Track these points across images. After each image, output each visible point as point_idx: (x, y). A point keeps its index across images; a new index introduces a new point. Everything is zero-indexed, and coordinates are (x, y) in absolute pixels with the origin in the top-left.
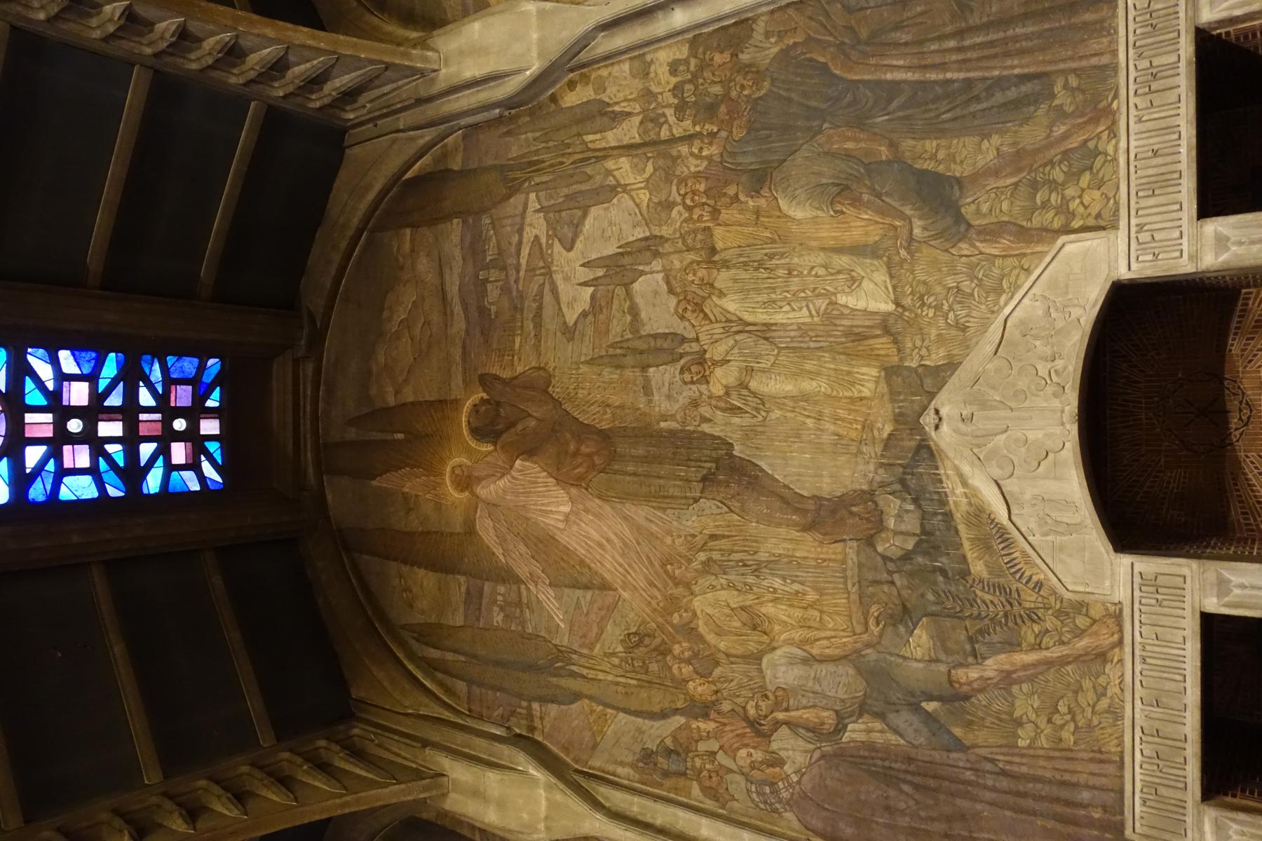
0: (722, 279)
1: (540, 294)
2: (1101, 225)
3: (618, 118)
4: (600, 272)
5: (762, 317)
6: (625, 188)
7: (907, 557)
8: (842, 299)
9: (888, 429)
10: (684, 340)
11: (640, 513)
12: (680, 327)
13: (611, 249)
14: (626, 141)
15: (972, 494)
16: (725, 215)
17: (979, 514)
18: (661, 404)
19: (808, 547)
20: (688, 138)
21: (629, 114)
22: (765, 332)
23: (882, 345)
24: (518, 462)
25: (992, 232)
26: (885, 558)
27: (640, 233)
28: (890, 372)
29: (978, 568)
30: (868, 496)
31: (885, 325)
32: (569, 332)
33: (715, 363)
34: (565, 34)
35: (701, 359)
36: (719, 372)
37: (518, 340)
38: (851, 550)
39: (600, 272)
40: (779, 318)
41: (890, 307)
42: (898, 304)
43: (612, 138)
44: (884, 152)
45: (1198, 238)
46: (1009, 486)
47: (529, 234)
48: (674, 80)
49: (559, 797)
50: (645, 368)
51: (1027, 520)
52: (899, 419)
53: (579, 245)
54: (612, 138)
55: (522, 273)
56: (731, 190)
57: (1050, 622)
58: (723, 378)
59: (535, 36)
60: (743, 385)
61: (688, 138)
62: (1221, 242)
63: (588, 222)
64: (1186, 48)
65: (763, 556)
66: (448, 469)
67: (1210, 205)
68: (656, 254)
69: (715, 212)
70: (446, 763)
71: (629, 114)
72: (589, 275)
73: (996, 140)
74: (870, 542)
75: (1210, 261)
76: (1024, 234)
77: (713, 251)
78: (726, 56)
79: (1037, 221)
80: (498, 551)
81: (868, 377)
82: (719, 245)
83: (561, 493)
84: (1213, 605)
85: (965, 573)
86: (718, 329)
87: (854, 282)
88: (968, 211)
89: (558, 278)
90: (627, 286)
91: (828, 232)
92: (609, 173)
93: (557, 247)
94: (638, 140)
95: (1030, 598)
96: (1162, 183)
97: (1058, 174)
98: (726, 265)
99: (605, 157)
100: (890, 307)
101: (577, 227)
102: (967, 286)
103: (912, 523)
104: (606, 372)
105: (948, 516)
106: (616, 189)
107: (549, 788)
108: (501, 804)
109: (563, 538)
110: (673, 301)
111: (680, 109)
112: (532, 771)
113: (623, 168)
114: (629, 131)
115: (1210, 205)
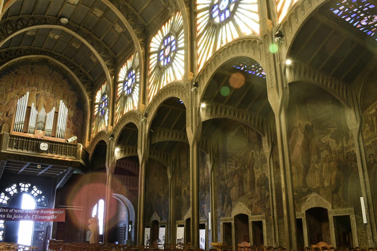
0: (327, 164)
1: (324, 133)
2: (333, 208)
3: (347, 142)
4: (327, 144)
5: (323, 170)
6: (338, 146)
7: (302, 192)
8: (326, 180)
9: (313, 188)
10: (320, 159)
11: (301, 157)
12: (321, 158)
13: (330, 145)
14: (344, 144)
15: (308, 197)
16: (334, 163)
17: (307, 198)
18: (313, 157)
19: (301, 180)
20: (344, 156)
21: (347, 144)
22: (322, 171)
23: (321, 186)
24: (303, 135)
25: (333, 197)
26: (301, 189)
27: (332, 150)
28: (319, 187)
29: (302, 199)
30: (307, 186)
31: (323, 186)
32: (320, 140)
33: (318, 164)
34: (354, 133)
35: (318, 162)
36: (317, 165)
37: (318, 130)
38: (301, 185)
39: (327, 144)
40: (323, 173)
41: (325, 186)
42: (326, 187)
43: (344, 142)
44: (341, 184)
45: (331, 216)
46: (309, 201)
47: (331, 129)
48: (351, 151)
49: (269, 153)
50: (317, 154)
51: (307, 203)
52: (314, 189)
53: (331, 139)
54: (344, 142)
55: (326, 129)
56: (337, 163)
57: (299, 206)
58: (316, 165)
59: (354, 128)
60: (316, 169)
61: (344, 156)
62: (331, 218)
63: (333, 140)
64: (348, 214)
65: (299, 175)
66: (301, 121)
67: (334, 217)
68: (330, 153)
69: (335, 161)
70: (266, 136)
71: (347, 144)
72: (327, 142)
73: (341, 196)
74: (303, 187)
75: (329, 217)
76: (332, 200)
77: (330, 162)
78: (353, 159)
79: (334, 201)
80: (292, 134)
81: (318, 185)
82: (331, 162)
83: (301, 143)
84: (303, 219)
85: (302, 197)
86: (322, 164)
87: (327, 182)
88: (335, 194)
89: (326, 136)
90: (326, 149)
91: (333, 177)
92: (340, 142)
93: (330, 135)
94: (344, 146)
95: (301, 204)
96: (336, 213)
97: (338, 203)
98: (329, 164)
99: (342, 141)
100: (325, 186)
101: (333, 138)
102: (327, 195)
103: (305, 192)
104: (315, 148)
105: (306, 195)
106: (338, 144)
107: (269, 152)
108: (265, 146)
109: (296, 145)
110: (324, 157)
111: (347, 153)
112: (270, 149)
113: (340, 145)
114: (345, 145)
115: (334, 217)
